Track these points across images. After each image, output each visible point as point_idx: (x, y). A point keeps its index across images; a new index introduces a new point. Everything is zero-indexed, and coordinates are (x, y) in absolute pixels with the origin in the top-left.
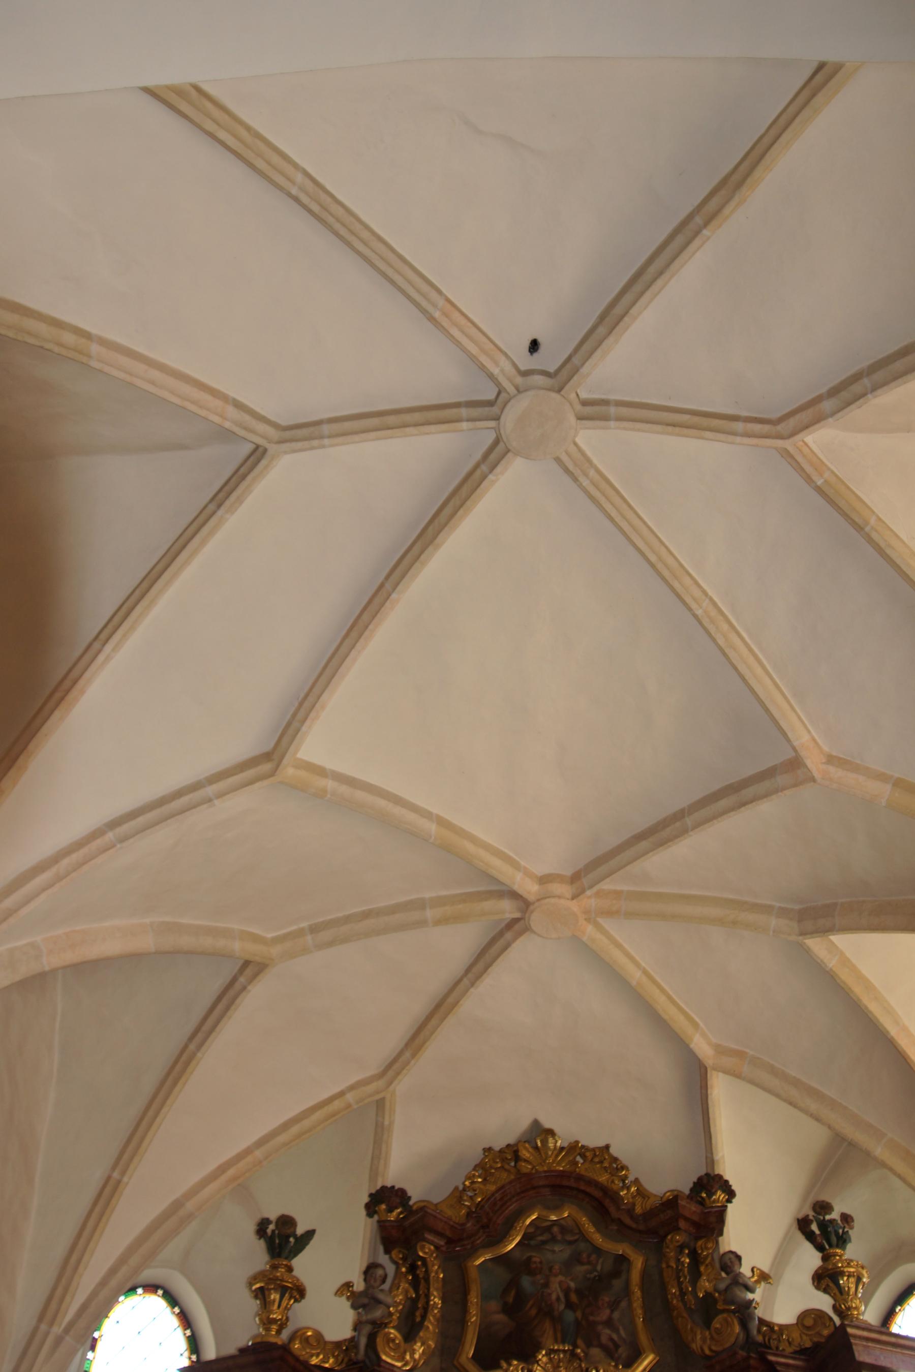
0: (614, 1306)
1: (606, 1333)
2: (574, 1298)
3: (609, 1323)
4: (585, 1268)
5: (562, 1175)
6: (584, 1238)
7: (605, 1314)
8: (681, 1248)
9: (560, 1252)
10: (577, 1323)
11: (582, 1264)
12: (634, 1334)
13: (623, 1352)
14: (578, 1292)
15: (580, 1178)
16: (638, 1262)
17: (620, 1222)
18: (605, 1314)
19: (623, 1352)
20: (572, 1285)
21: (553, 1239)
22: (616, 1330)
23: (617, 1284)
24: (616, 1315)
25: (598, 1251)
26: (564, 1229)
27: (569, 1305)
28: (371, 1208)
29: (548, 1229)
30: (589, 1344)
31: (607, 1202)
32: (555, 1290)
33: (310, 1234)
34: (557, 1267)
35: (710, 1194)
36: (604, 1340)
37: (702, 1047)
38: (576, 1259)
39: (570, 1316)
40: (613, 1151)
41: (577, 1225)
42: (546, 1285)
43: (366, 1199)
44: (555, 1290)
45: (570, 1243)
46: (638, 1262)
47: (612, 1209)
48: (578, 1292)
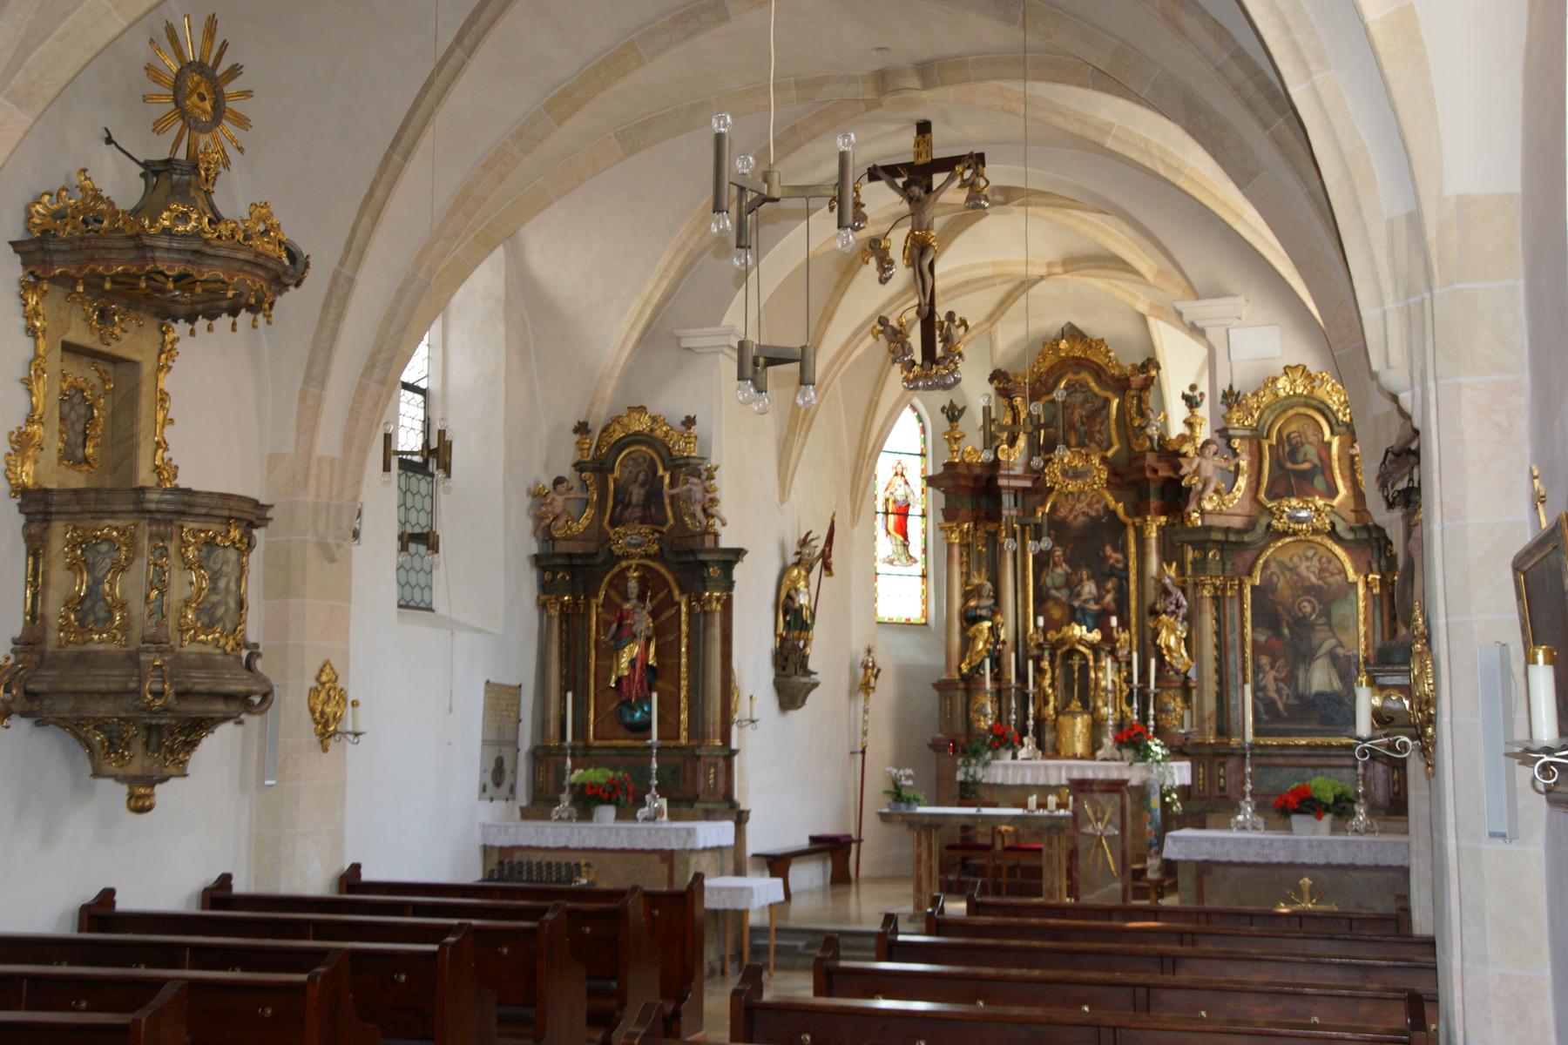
0: (1102, 423)
1: (1098, 436)
2: (1085, 420)
3: (1099, 431)
4: (1090, 405)
5: (1079, 358)
6: (1090, 389)
7: (1097, 428)
8: (1133, 397)
9: (1079, 397)
10: (1086, 432)
11: (1088, 403)
12: (1110, 436)
13: (1105, 445)
14: (1087, 418)
15: (1088, 360)
16: (1115, 403)
17: (1106, 382)
18: (1097, 428)
19: (1105, 445)
20: (1084, 413)
21: (1076, 391)
22: (1102, 434)
23: (1104, 412)
24: (1103, 428)
25: (1096, 396)
26: (1081, 386)
27: (1083, 423)
28: (992, 379)
29: (1074, 385)
30: (1090, 441)
31: (1101, 373)
32: (1076, 417)
33: (964, 408)
34: (1077, 405)
35: (1148, 371)
36: (1097, 439)
37: (1142, 307)
38: (1086, 401)
39: (1082, 429)
40: (1106, 342)
41: (1087, 383)
42: (1072, 414)
43: (988, 377)
44: (1076, 417)
45: (1084, 392)
46: (1115, 403)
47: (1103, 376)
48: (1087, 418)
